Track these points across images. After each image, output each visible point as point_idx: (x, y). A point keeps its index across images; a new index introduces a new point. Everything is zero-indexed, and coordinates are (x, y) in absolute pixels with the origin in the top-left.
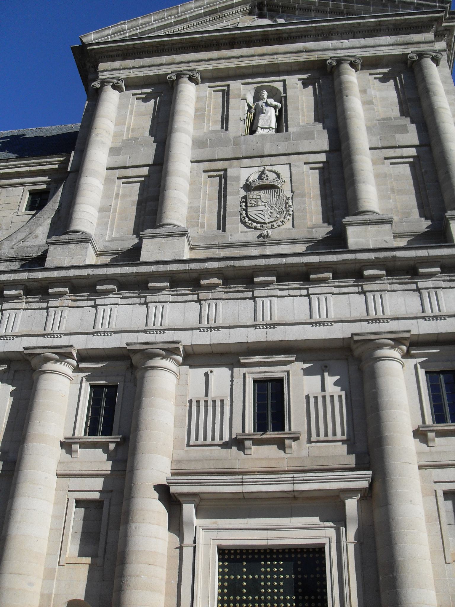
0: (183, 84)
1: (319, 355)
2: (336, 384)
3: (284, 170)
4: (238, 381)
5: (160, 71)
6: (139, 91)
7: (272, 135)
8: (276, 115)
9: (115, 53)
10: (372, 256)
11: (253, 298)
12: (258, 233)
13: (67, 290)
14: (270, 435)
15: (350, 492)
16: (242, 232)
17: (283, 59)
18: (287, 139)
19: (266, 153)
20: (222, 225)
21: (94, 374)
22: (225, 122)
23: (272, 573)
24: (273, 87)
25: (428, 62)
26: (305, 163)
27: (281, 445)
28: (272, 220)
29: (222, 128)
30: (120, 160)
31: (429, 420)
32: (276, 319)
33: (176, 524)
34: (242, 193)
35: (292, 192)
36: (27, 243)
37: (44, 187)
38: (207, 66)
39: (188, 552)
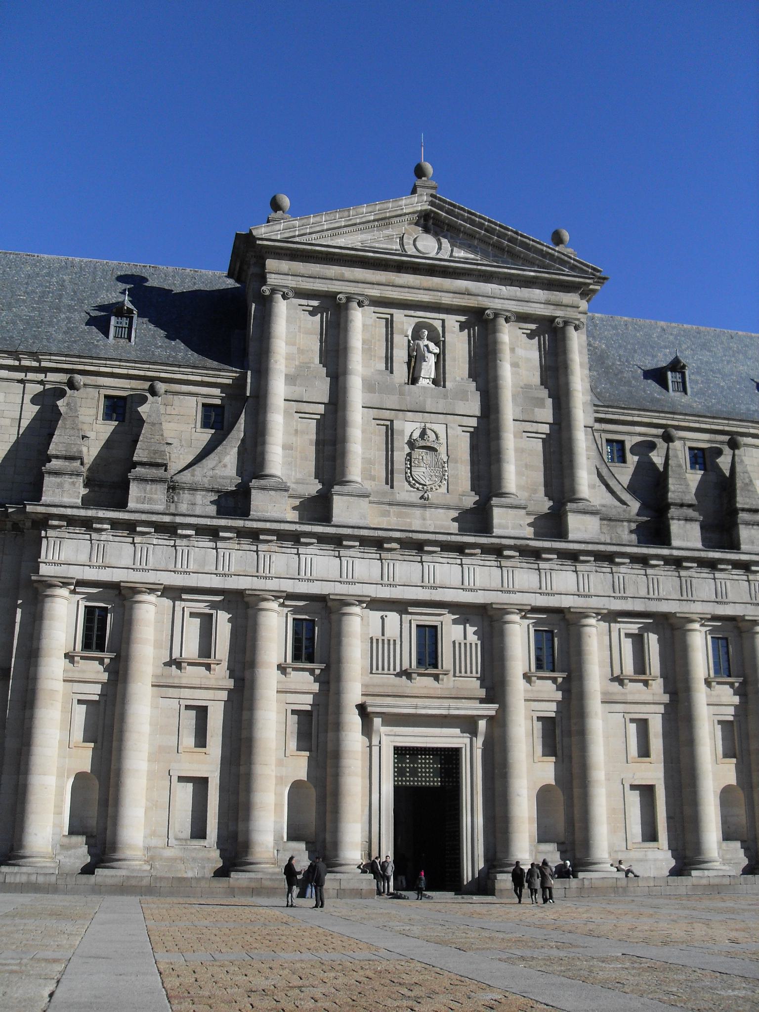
1: (465, 612)
2: (475, 633)
3: (440, 429)
4: (406, 626)
6: (304, 302)
7: (432, 389)
9: (283, 252)
11: (422, 562)
12: (421, 494)
13: (275, 538)
15: (481, 717)
17: (447, 299)
18: (445, 397)
20: (390, 480)
21: (296, 610)
22: (389, 360)
23: (425, 763)
25: (571, 330)
27: (436, 677)
29: (387, 368)
30: (298, 391)
32: (438, 582)
33: (367, 730)
34: (407, 450)
37: (218, 402)
38: (375, 292)
39: (375, 750)
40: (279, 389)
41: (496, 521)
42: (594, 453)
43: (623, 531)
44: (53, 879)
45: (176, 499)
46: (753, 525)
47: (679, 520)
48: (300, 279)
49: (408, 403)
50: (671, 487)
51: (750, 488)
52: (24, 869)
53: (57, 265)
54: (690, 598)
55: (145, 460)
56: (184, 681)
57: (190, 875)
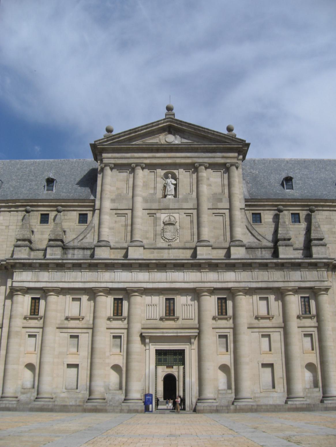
0: (138, 170)
5: (128, 161)
7: (173, 199)
8: (174, 188)
10: (204, 261)
14: (171, 317)
16: (162, 243)
17: (178, 161)
18: (178, 201)
19: (171, 208)
24: (173, 172)
26: (184, 213)
28: (172, 238)
31: (217, 315)
35: (180, 226)
36: (83, 241)
38: (147, 161)
40: (107, 205)
41: (198, 252)
42: (245, 220)
43: (258, 252)
44: (15, 406)
45: (67, 252)
46: (319, 246)
47: (283, 246)
48: (116, 159)
49: (162, 206)
50: (280, 232)
51: (318, 229)
52: (4, 402)
53: (30, 163)
54: (289, 280)
55: (53, 238)
56: (69, 326)
57: (71, 404)
